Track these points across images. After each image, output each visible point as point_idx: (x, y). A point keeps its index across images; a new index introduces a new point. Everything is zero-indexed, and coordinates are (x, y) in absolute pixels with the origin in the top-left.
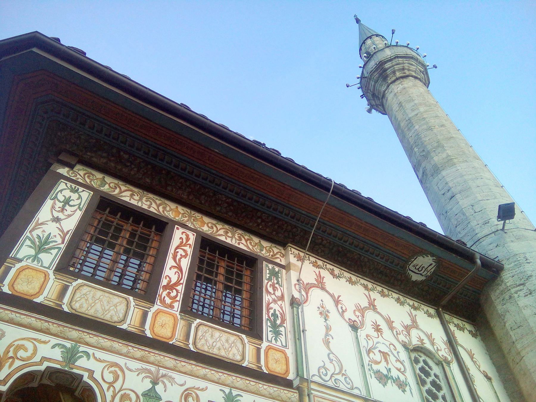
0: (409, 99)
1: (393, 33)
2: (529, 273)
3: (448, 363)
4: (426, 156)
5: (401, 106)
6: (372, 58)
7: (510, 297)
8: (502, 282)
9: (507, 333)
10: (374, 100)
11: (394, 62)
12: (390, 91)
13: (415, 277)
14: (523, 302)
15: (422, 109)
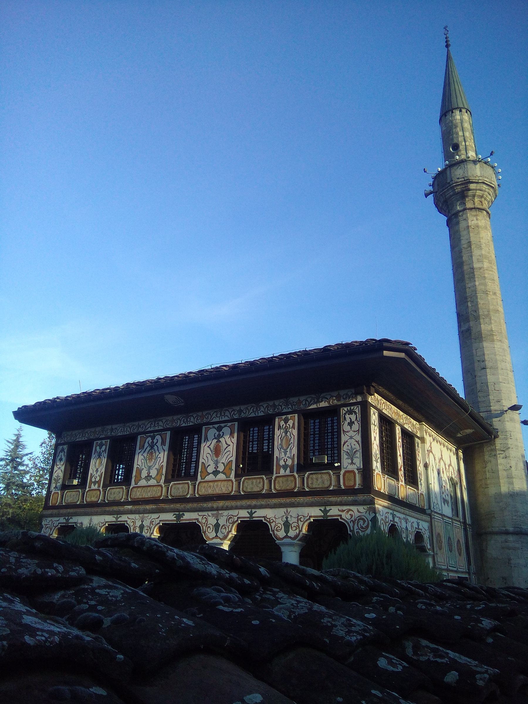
0: (479, 243)
1: (491, 154)
2: (509, 445)
3: (457, 484)
4: (477, 318)
5: (470, 246)
6: (462, 165)
7: (495, 455)
8: (495, 444)
9: (485, 472)
10: (443, 204)
11: (479, 186)
12: (464, 216)
13: (459, 435)
14: (500, 461)
15: (486, 265)
